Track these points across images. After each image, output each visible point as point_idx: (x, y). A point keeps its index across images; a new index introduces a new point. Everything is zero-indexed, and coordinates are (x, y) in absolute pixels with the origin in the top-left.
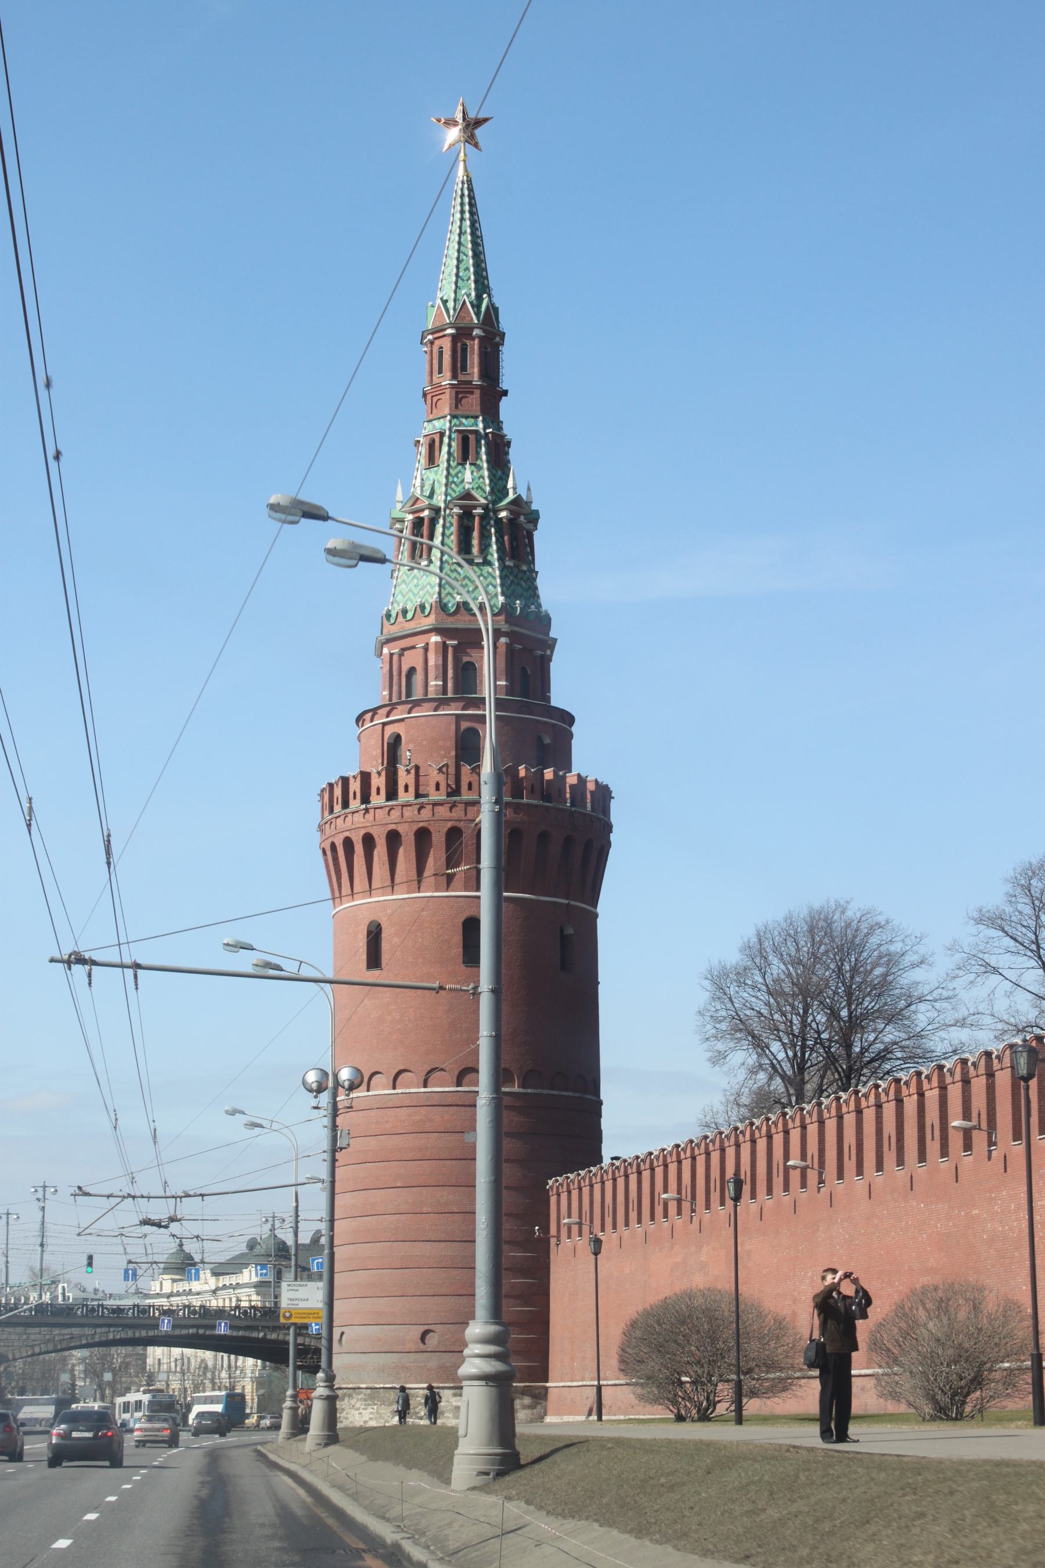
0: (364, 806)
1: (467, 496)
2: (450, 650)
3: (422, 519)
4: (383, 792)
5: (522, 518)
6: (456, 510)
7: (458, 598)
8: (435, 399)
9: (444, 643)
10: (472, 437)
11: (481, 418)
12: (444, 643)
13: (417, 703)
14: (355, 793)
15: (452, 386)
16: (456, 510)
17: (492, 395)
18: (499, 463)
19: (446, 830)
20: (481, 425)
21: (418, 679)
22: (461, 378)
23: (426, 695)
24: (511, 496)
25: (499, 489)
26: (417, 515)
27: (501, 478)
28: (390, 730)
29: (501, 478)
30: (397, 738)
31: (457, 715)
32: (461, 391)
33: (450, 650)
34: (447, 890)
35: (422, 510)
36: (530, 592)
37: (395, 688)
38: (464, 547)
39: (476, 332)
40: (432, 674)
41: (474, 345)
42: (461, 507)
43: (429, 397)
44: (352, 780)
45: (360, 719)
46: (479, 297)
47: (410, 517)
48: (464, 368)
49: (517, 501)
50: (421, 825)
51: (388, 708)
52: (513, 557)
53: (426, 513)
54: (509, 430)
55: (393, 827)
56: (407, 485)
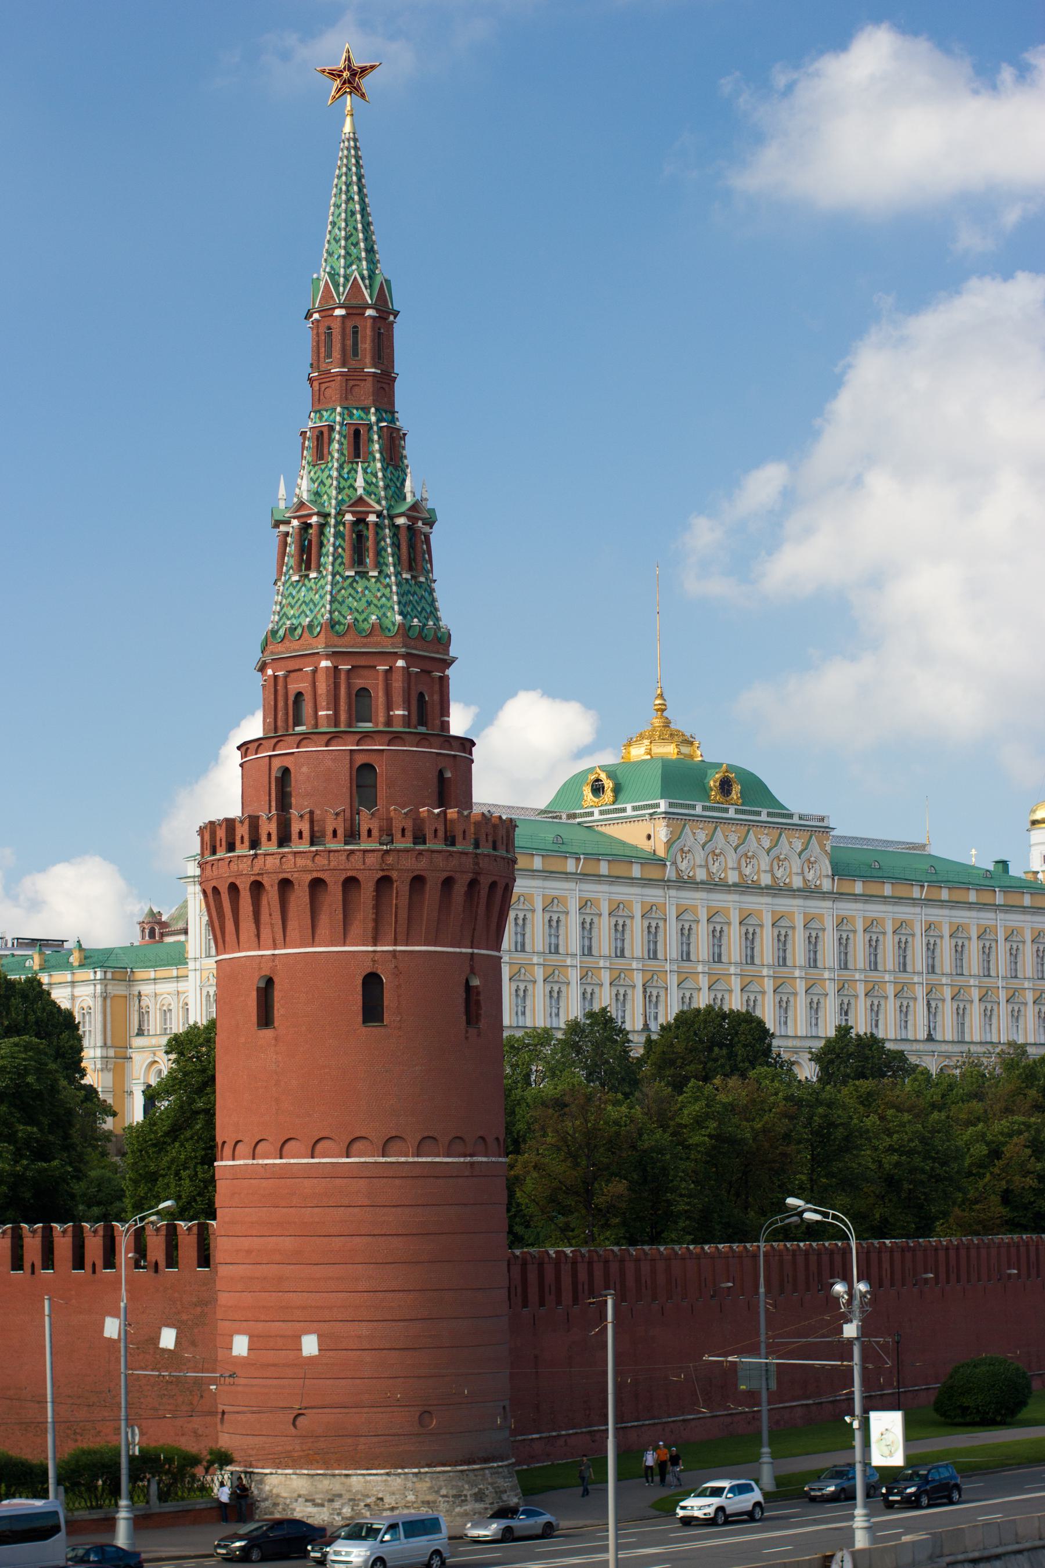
0: (252, 852)
1: (360, 500)
2: (343, 676)
3: (310, 525)
4: (274, 837)
5: (420, 524)
6: (349, 517)
8: (324, 386)
9: (336, 668)
11: (373, 410)
12: (336, 668)
13: (305, 737)
14: (242, 837)
15: (341, 374)
16: (349, 517)
17: (385, 383)
19: (342, 879)
20: (373, 419)
21: (307, 709)
22: (353, 364)
23: (316, 726)
26: (303, 520)
28: (277, 764)
30: (286, 771)
31: (351, 750)
32: (351, 379)
33: (343, 676)
35: (310, 516)
37: (280, 714)
38: (358, 557)
39: (369, 312)
40: (322, 702)
41: (365, 328)
42: (353, 513)
43: (316, 384)
44: (238, 825)
49: (415, 507)
51: (276, 740)
52: (410, 569)
53: (314, 520)
54: (404, 421)
56: (291, 485)
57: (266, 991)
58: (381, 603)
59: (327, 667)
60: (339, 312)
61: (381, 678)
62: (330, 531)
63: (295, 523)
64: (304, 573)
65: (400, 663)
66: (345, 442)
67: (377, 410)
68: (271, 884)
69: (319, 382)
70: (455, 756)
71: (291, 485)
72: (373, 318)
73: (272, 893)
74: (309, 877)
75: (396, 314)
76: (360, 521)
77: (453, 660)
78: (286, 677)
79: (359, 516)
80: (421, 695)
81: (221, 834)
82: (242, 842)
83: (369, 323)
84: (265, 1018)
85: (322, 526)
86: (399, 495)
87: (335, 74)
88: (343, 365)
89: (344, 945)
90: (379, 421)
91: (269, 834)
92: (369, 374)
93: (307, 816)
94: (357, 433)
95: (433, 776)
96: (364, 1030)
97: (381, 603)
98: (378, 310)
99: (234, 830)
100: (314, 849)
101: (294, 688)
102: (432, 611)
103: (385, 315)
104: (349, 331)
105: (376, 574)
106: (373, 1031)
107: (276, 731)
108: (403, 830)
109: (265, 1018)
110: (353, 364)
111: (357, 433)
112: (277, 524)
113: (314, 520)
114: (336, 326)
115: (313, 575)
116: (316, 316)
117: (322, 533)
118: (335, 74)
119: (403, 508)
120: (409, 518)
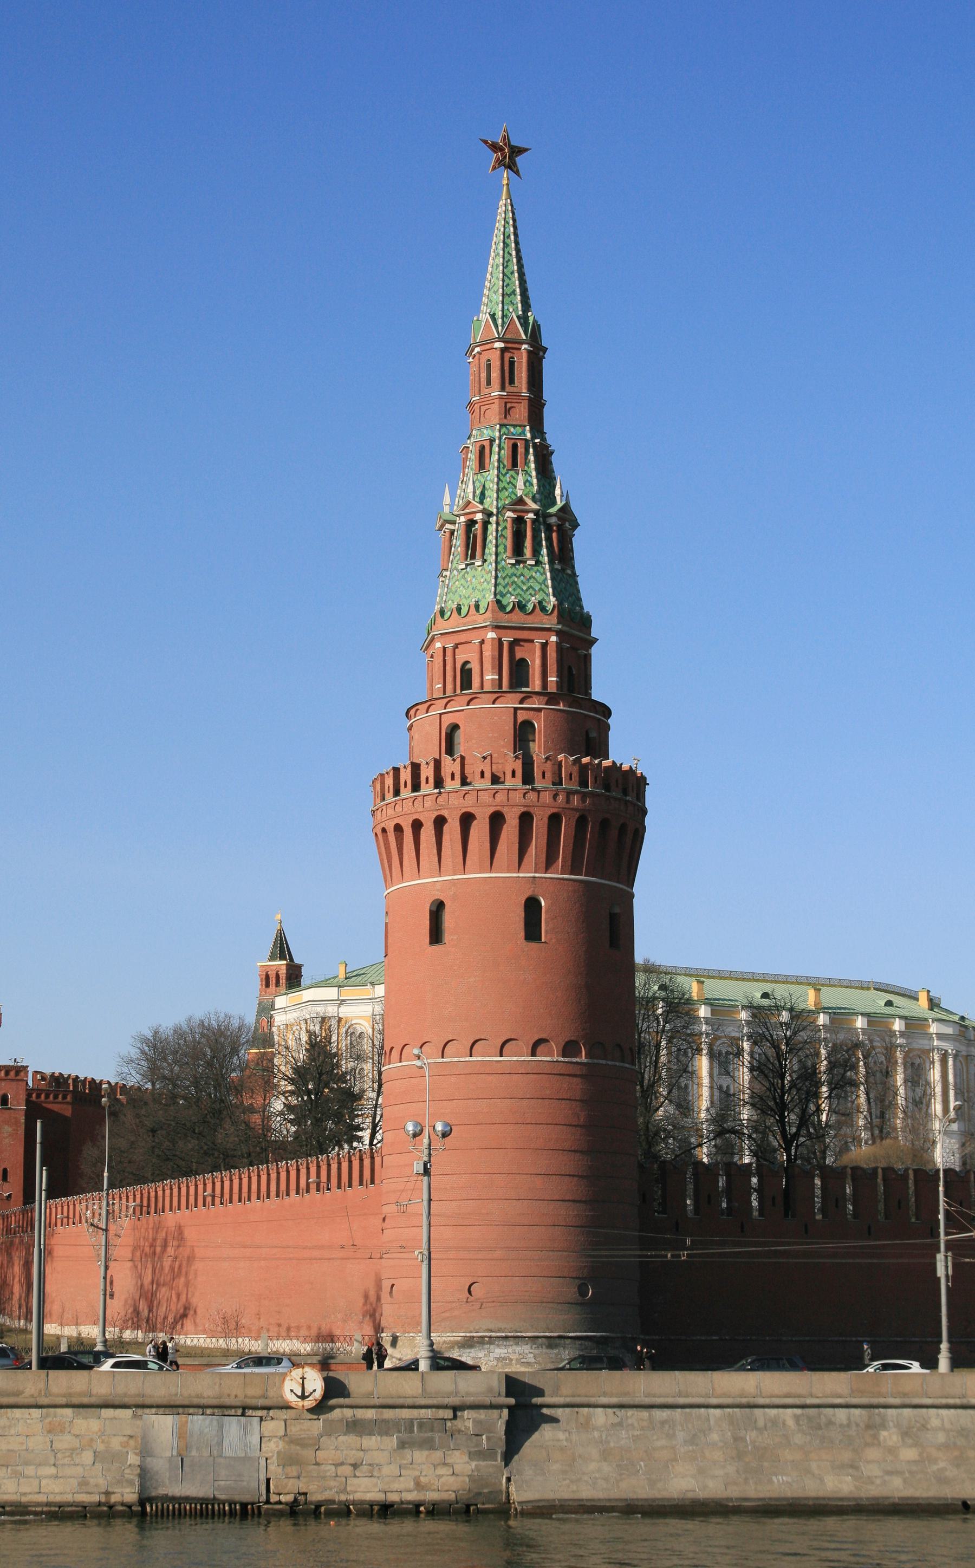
1: (520, 501)
3: (476, 522)
11: (528, 428)
15: (501, 397)
20: (529, 436)
24: (559, 504)
34: (491, 871)
35: (475, 513)
38: (518, 550)
57: (437, 910)
62: (492, 528)
63: (463, 519)
64: (469, 561)
70: (599, 720)
73: (452, 830)
75: (545, 350)
76: (519, 521)
77: (595, 640)
80: (570, 668)
84: (436, 935)
85: (486, 524)
87: (495, 147)
90: (533, 437)
91: (427, 779)
101: (460, 659)
102: (577, 600)
106: (534, 945)
107: (444, 693)
109: (436, 935)
110: (509, 388)
113: (479, 517)
117: (485, 529)
118: (495, 147)
120: (559, 519)
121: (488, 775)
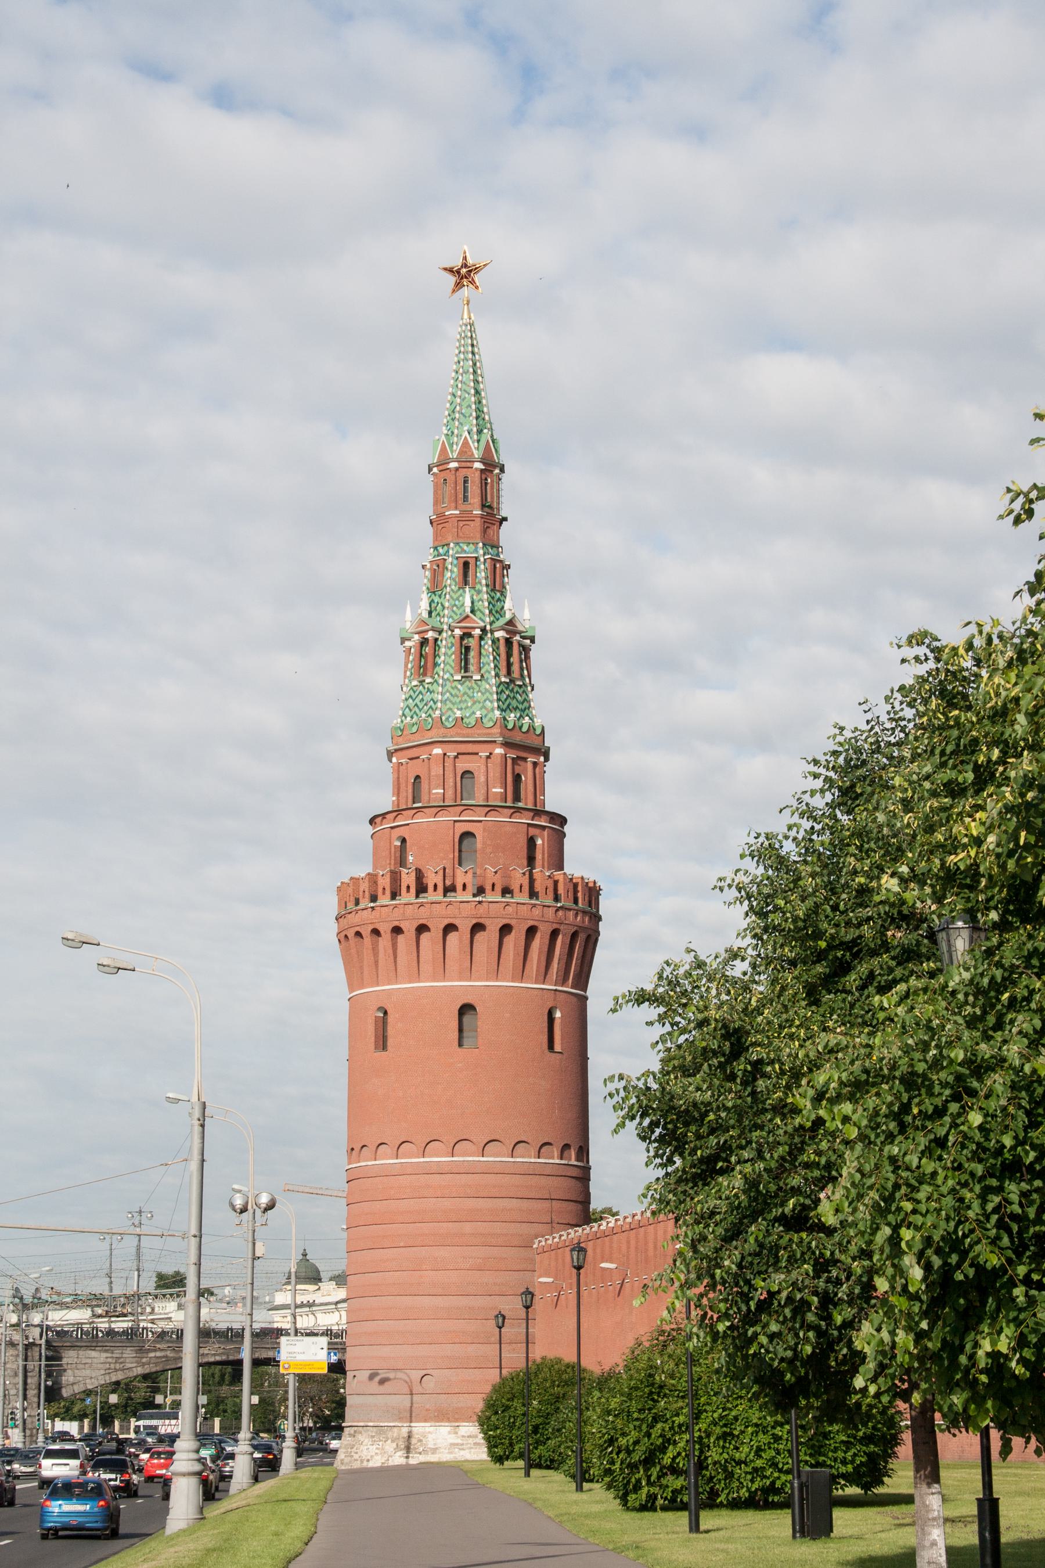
0: (372, 905)
3: (427, 639)
7: (458, 714)
10: (472, 562)
11: (481, 545)
15: (456, 516)
16: (458, 632)
18: (497, 587)
19: (443, 926)
20: (481, 552)
22: (464, 507)
24: (508, 616)
25: (496, 611)
26: (422, 635)
27: (499, 600)
29: (499, 600)
36: (526, 704)
43: (435, 524)
45: (372, 821)
46: (480, 432)
47: (416, 637)
48: (465, 498)
49: (511, 623)
50: (421, 922)
51: (395, 814)
55: (396, 923)
56: (415, 607)
58: (478, 702)
59: (437, 755)
60: (453, 465)
61: (483, 761)
63: (416, 637)
65: (499, 751)
66: (455, 570)
67: (484, 544)
68: (366, 931)
69: (438, 522)
71: (415, 607)
72: (482, 470)
74: (416, 924)
76: (467, 635)
78: (456, 757)
79: (466, 631)
81: (365, 886)
82: (384, 893)
83: (478, 474)
86: (501, 612)
88: (456, 508)
89: (497, 980)
90: (484, 554)
92: (476, 516)
93: (441, 873)
94: (466, 565)
95: (523, 842)
96: (460, 1050)
97: (473, 702)
98: (484, 464)
99: (376, 883)
100: (394, 902)
103: (492, 467)
104: (461, 481)
105: (479, 678)
108: (493, 885)
110: (464, 507)
111: (466, 565)
112: (403, 640)
113: (430, 635)
114: (450, 478)
115: (428, 680)
116: (435, 470)
119: (502, 622)
120: (508, 632)
121: (498, 888)
